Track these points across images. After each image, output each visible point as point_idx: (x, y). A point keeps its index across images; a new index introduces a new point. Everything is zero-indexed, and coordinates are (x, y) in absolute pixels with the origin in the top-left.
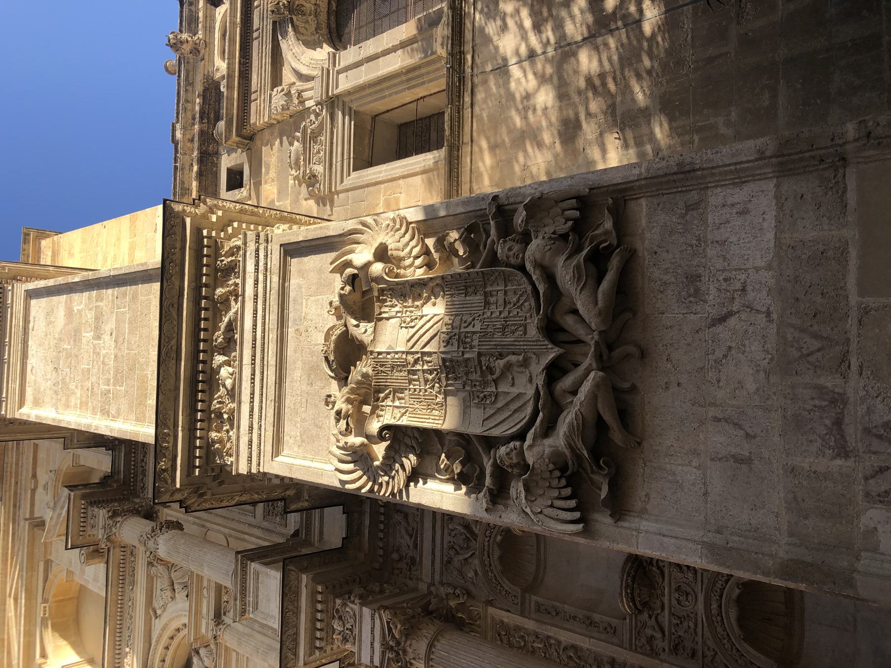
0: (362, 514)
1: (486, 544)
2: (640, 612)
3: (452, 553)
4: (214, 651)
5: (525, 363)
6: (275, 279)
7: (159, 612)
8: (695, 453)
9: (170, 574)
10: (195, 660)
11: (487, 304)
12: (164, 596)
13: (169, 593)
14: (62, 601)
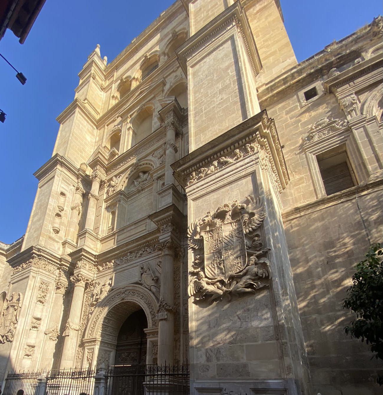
10: (147, 174)
13: (159, 156)
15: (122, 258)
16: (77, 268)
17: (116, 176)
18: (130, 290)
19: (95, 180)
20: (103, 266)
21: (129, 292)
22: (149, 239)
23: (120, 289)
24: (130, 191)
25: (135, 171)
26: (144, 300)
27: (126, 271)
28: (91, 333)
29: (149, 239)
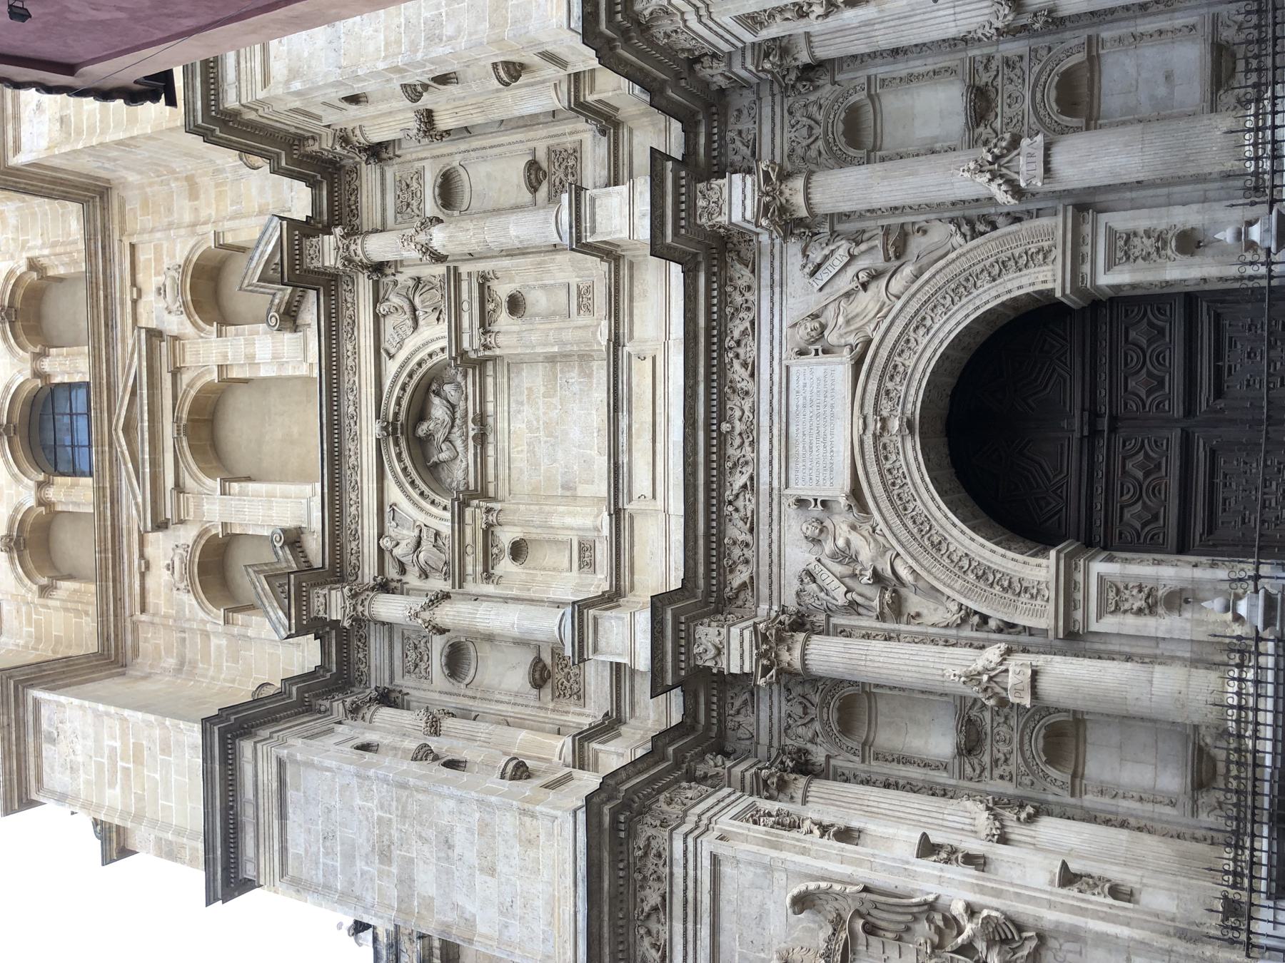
0: (697, 135)
1: (830, 125)
2: (978, 126)
3: (794, 144)
4: (463, 384)
7: (392, 351)
12: (400, 332)
14: (197, 421)
19: (366, 603)
21: (888, 393)
24: (462, 483)
25: (403, 444)
26: (936, 320)
27: (793, 429)
28: (1028, 595)
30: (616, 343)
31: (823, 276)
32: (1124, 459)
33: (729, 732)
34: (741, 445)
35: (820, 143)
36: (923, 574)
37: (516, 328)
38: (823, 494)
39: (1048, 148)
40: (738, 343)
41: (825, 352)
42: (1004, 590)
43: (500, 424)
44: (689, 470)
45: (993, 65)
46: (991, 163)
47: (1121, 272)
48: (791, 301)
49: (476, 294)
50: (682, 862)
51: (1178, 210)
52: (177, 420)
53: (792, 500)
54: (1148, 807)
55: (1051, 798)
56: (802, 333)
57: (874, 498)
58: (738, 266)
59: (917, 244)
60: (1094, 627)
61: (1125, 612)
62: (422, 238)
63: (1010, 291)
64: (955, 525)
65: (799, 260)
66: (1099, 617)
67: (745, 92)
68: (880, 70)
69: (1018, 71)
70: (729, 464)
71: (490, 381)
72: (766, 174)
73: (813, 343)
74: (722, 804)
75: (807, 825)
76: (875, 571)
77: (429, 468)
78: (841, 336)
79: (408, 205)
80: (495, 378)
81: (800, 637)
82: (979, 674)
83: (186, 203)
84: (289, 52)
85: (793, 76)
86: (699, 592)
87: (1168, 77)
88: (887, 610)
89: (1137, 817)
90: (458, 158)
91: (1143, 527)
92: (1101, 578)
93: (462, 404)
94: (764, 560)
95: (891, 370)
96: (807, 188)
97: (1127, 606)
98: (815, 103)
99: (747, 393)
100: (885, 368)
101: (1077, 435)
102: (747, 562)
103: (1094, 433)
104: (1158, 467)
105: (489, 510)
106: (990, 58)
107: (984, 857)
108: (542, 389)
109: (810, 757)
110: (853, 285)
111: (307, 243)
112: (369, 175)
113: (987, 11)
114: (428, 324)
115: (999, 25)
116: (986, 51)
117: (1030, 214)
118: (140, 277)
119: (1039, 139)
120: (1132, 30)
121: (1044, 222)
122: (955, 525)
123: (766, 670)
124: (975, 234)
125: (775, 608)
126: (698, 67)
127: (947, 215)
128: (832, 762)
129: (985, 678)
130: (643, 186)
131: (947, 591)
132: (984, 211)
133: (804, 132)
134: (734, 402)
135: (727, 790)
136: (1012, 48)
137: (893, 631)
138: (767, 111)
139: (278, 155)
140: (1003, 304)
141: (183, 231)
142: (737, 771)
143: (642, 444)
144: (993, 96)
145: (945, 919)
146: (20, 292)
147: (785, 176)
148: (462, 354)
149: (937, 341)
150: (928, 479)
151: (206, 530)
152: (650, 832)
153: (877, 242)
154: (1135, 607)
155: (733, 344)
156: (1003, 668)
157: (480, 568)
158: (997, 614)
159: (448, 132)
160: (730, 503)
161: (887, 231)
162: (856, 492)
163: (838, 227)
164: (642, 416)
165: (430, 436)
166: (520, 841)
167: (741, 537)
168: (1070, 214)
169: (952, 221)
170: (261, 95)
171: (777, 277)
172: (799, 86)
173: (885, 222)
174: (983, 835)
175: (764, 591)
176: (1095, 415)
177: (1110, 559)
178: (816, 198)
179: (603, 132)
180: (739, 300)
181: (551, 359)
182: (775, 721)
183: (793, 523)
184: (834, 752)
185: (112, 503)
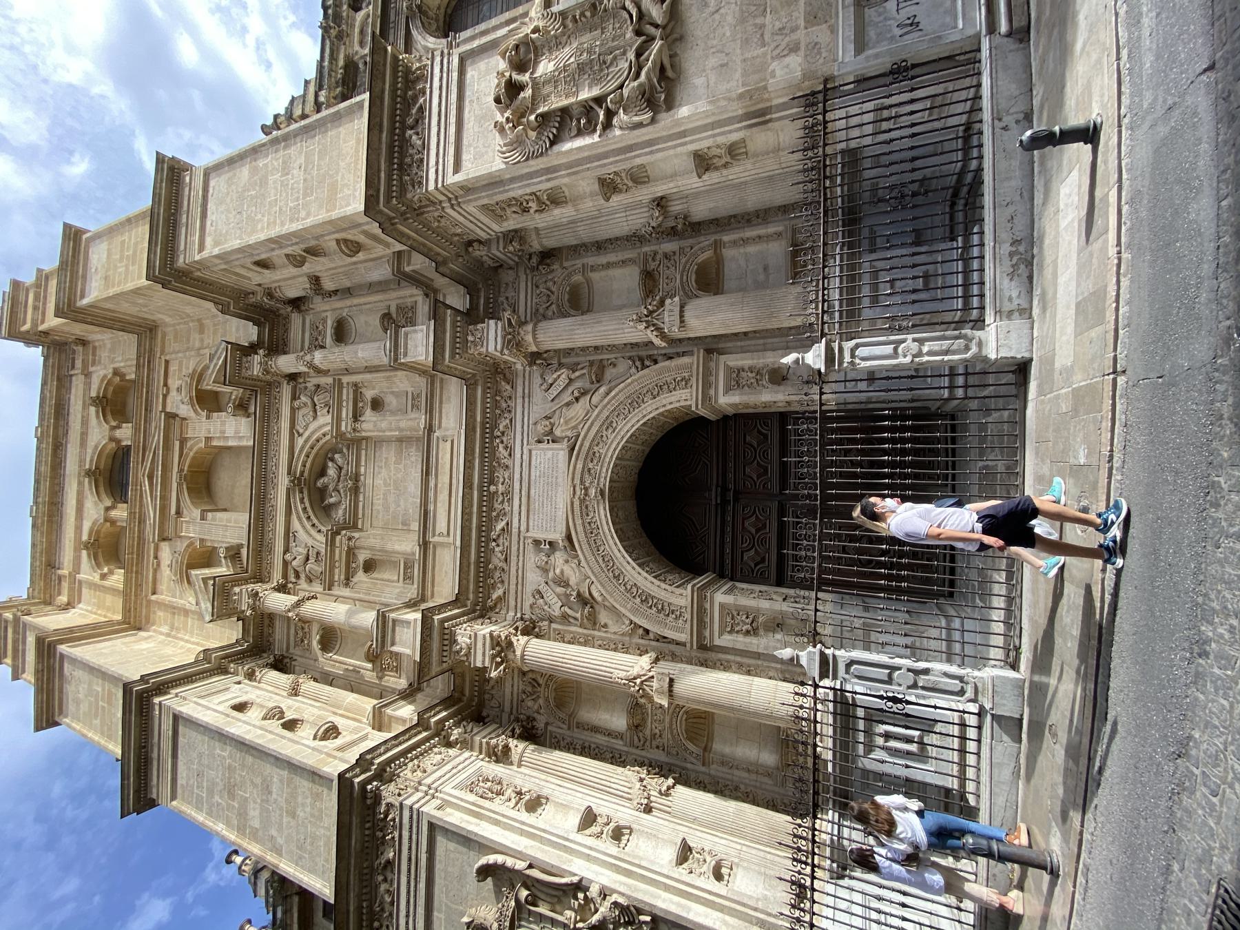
0: (479, 298)
5: (624, 53)
6: (455, 75)
8: (704, 71)
9: (312, 400)
10: (330, 464)
11: (603, 33)
15: (494, 514)
16: (468, 655)
17: (287, 550)
18: (583, 468)
20: (494, 586)
21: (589, 470)
22: (479, 419)
23: (572, 503)
25: (306, 492)
27: (532, 492)
29: (479, 419)
30: (430, 429)
31: (554, 392)
32: (744, 519)
33: (487, 702)
34: (502, 502)
35: (554, 306)
36: (608, 597)
37: (374, 419)
38: (551, 536)
39: (682, 307)
40: (503, 433)
41: (553, 441)
42: (659, 611)
43: (367, 480)
44: (466, 517)
45: (658, 257)
46: (647, 316)
47: (733, 395)
48: (535, 407)
49: (351, 396)
50: (408, 827)
51: (769, 354)
52: (180, 471)
53: (530, 541)
54: (754, 776)
55: (689, 766)
56: (540, 428)
57: (579, 541)
58: (503, 383)
59: (610, 373)
60: (717, 642)
61: (738, 632)
62: (308, 358)
63: (664, 406)
64: (628, 563)
65: (538, 380)
66: (721, 634)
67: (510, 272)
68: (591, 260)
69: (672, 262)
70: (494, 514)
71: (363, 452)
72: (509, 320)
73: (547, 435)
74: (455, 771)
75: (509, 792)
76: (579, 595)
77: (324, 508)
78: (562, 431)
79: (317, 339)
80: (366, 450)
81: (523, 639)
82: (635, 678)
83: (197, 336)
84: (215, 231)
85: (534, 260)
86: (469, 603)
87: (766, 268)
88: (585, 620)
89: (746, 785)
90: (346, 310)
91: (756, 565)
92: (722, 606)
93: (345, 466)
94: (513, 581)
95: (591, 456)
96: (534, 331)
97: (737, 629)
98: (551, 280)
99: (507, 466)
100: (587, 453)
101: (714, 503)
102: (502, 582)
103: (725, 502)
104: (764, 526)
105: (350, 539)
106: (655, 253)
107: (630, 828)
108: (394, 459)
109: (535, 723)
110: (570, 399)
111: (244, 359)
112: (296, 320)
113: (646, 215)
114: (323, 415)
115: (654, 224)
116: (653, 248)
117: (679, 355)
118: (170, 381)
119: (677, 299)
120: (742, 235)
121: (685, 360)
122: (628, 563)
123: (498, 665)
124: (644, 367)
125: (519, 615)
126: (470, 249)
127: (628, 354)
128: (549, 728)
129: (638, 681)
130: (432, 322)
131: (622, 610)
132: (651, 353)
133: (544, 298)
134: (501, 474)
135: (467, 754)
136: (669, 246)
137: (590, 635)
138: (523, 285)
139: (229, 303)
140: (661, 414)
141: (193, 353)
142: (477, 738)
143: (443, 496)
144: (657, 277)
145: (586, 897)
146: (111, 389)
147: (522, 324)
148: (340, 435)
149: (619, 437)
150: (613, 530)
151: (191, 544)
152: (389, 800)
153: (584, 371)
154: (744, 628)
155: (499, 434)
156: (651, 674)
157: (343, 577)
158: (654, 628)
159: (336, 292)
160: (494, 540)
161: (592, 363)
162: (569, 538)
163: (563, 361)
164: (444, 479)
165: (325, 487)
166: (312, 794)
167: (500, 565)
168: (701, 355)
169: (630, 358)
170: (197, 258)
171: (526, 391)
172: (540, 267)
173: (591, 358)
174: (635, 803)
175: (512, 603)
176: (725, 489)
177: (730, 591)
178: (541, 337)
179: (427, 295)
180: (504, 405)
181: (400, 440)
182: (515, 696)
183: (532, 556)
184: (551, 720)
185: (139, 523)
